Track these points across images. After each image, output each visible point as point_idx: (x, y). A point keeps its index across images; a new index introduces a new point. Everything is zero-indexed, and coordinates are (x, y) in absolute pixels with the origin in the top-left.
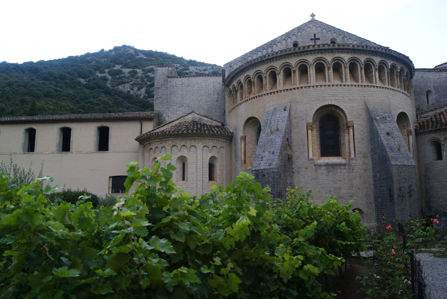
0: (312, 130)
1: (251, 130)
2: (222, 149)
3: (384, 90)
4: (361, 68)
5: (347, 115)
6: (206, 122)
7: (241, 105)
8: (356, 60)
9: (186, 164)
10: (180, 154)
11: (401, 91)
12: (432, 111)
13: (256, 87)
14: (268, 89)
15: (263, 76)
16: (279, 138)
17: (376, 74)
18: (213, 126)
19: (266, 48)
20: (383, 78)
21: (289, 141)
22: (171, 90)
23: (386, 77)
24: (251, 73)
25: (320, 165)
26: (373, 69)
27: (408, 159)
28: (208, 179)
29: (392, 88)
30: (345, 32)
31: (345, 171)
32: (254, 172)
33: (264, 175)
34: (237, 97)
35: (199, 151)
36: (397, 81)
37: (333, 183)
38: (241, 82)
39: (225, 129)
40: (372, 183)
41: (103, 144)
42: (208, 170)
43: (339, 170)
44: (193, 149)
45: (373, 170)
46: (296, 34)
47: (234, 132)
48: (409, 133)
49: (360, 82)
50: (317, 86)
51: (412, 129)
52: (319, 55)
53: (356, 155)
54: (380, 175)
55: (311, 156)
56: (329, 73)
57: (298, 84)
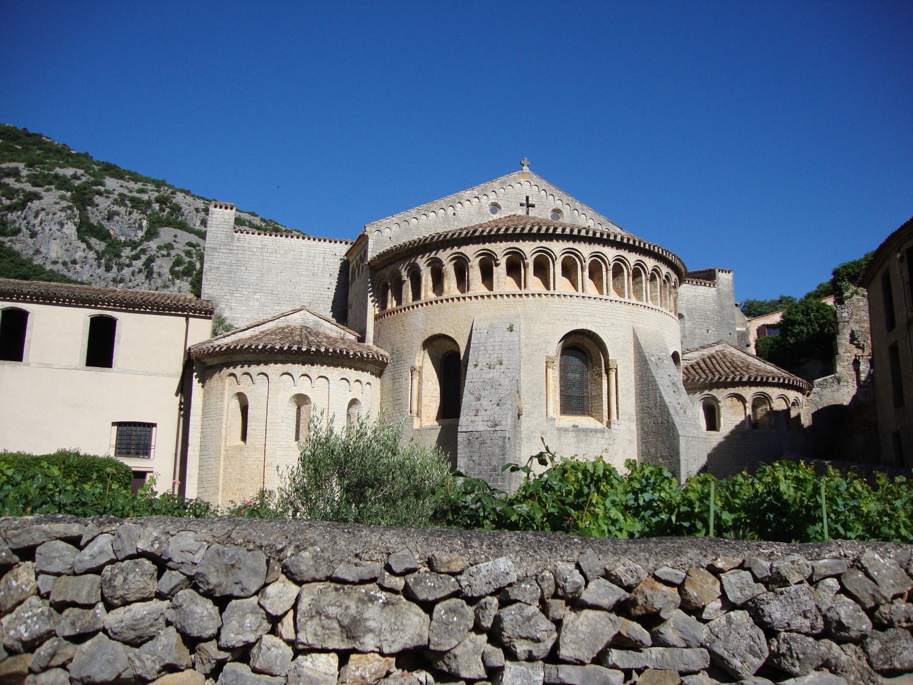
6: (328, 332)
12: (697, 350)
22: (240, 256)
25: (566, 430)
31: (603, 441)
33: (483, 443)
43: (595, 440)
49: (626, 297)
52: (571, 245)
53: (620, 417)
55: (551, 414)
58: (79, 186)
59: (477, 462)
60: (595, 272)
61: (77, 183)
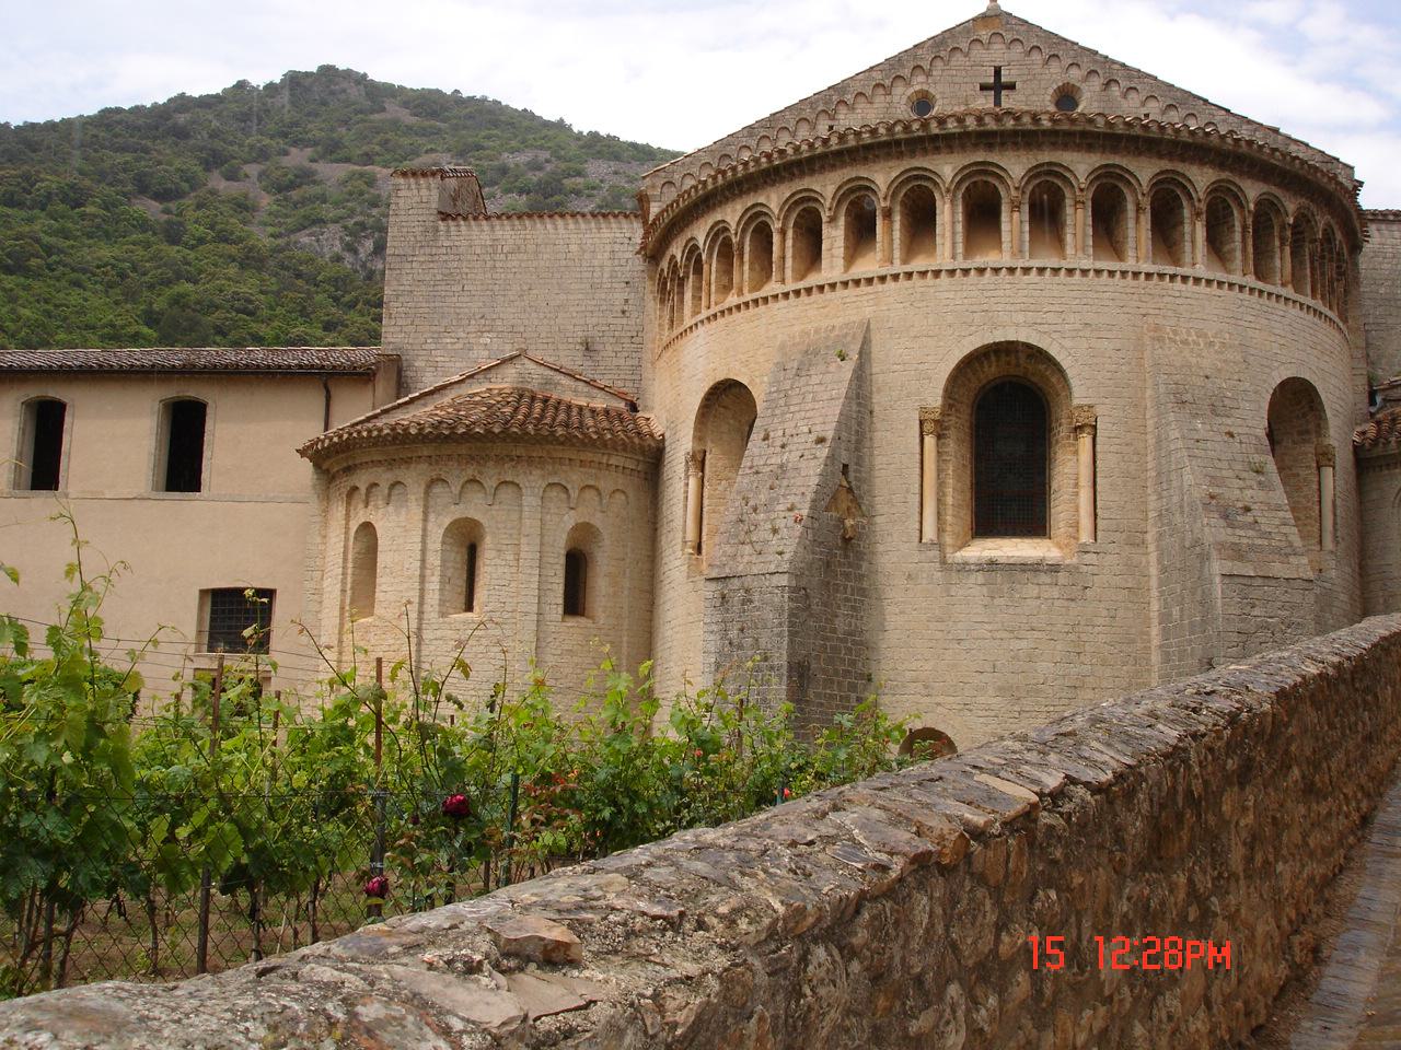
0: (939, 437)
1: (725, 428)
2: (620, 497)
3: (1225, 291)
4: (1139, 209)
5: (1074, 382)
6: (567, 397)
7: (695, 333)
8: (1120, 177)
9: (479, 553)
10: (457, 512)
11: (1301, 299)
13: (746, 267)
14: (789, 273)
15: (776, 226)
16: (813, 463)
17: (1195, 233)
18: (593, 411)
19: (807, 113)
20: (1226, 249)
21: (852, 475)
23: (1238, 244)
24: (731, 214)
25: (964, 567)
26: (1187, 213)
27: (1287, 555)
28: (560, 609)
29: (1260, 285)
30: (1114, 62)
31: (1055, 592)
32: (713, 586)
34: (682, 301)
35: (530, 500)
36: (1282, 261)
37: (1005, 635)
38: (696, 247)
39: (635, 420)
40: (1156, 642)
41: (182, 467)
42: (561, 572)
43: (1032, 591)
44: (506, 494)
45: (1162, 593)
46: (926, 66)
47: (667, 435)
48: (1324, 458)
50: (966, 272)
51: (1336, 444)
52: (980, 156)
54: (1182, 610)
55: (930, 533)
56: (1014, 223)
57: (897, 262)
58: (539, 183)
59: (735, 642)
60: (1046, 215)
61: (534, 177)
